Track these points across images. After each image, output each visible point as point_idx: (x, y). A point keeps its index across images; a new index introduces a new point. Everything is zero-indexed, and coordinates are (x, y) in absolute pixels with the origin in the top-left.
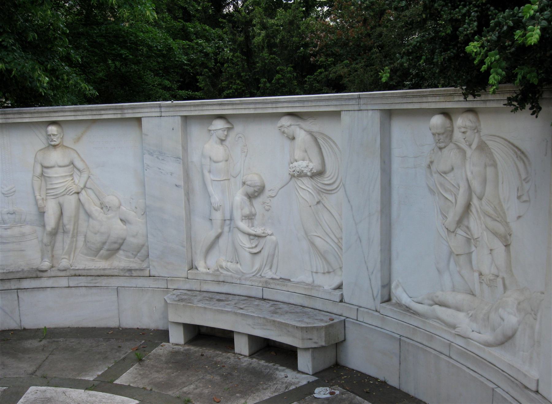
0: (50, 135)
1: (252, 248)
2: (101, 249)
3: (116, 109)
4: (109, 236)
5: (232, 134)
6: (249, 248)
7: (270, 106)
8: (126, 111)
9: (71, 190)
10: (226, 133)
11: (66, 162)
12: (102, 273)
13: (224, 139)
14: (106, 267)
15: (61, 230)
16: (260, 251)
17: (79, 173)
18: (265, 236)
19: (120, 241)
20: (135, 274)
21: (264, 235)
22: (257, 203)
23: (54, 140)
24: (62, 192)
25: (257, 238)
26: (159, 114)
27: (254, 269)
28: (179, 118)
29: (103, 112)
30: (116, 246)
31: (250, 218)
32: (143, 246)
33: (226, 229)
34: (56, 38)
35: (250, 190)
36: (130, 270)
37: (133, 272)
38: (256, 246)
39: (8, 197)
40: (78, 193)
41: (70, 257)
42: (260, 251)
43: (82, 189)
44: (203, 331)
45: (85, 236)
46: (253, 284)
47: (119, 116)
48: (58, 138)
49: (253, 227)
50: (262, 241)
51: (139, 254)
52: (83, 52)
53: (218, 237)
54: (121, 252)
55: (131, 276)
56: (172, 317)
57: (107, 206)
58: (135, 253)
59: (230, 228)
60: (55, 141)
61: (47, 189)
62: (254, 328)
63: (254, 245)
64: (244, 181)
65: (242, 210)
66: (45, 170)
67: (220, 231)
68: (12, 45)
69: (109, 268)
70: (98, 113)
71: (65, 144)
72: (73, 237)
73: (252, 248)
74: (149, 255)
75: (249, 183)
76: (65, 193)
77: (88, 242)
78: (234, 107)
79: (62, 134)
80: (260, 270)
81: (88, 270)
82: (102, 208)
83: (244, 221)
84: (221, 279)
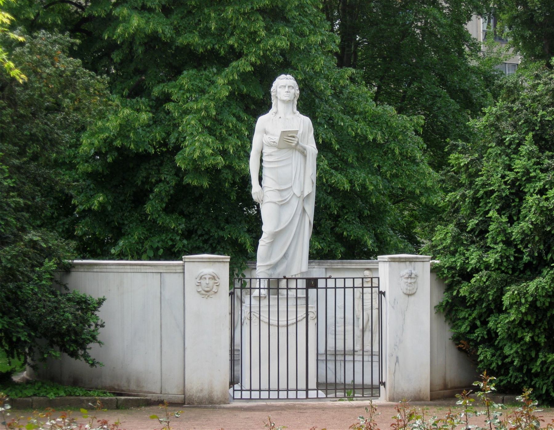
68: (353, 220)
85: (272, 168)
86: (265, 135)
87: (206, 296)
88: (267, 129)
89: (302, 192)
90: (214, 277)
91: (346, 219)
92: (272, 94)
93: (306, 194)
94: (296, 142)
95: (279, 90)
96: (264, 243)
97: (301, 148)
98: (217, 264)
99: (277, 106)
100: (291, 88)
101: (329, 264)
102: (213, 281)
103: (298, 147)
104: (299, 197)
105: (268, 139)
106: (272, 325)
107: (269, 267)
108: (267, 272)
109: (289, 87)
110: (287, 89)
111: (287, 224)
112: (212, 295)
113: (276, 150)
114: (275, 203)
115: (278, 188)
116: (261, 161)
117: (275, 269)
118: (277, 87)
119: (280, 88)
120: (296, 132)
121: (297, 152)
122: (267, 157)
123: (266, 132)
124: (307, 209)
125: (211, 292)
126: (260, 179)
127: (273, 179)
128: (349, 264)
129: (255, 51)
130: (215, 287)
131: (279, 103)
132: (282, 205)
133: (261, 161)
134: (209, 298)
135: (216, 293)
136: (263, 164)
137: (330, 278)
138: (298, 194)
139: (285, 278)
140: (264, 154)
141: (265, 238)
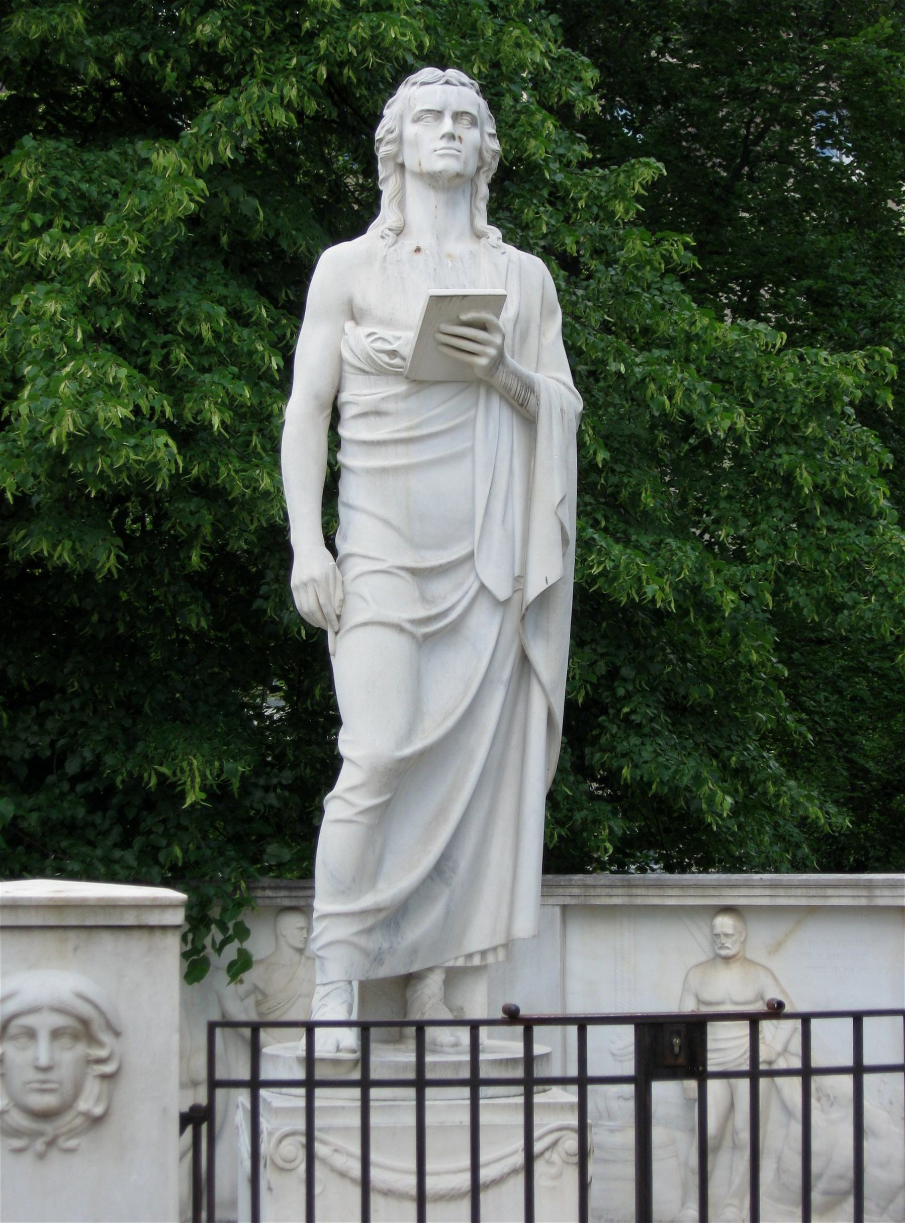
3: (856, 885)
8: (877, 892)
23: (727, 945)
24: (737, 1059)
29: (830, 892)
34: (754, 689)
39: (621, 1061)
45: (779, 1160)
47: (863, 902)
48: (736, 941)
52: (827, 699)
57: (829, 1096)
60: (728, 948)
68: (652, 720)
70: (820, 892)
71: (749, 955)
79: (744, 934)
85: (384, 470)
86: (349, 325)
87: (39, 1145)
88: (359, 301)
89: (520, 580)
90: (85, 1023)
91: (627, 719)
92: (382, 151)
93: (534, 589)
94: (492, 351)
95: (411, 130)
96: (347, 813)
97: (515, 385)
98: (108, 943)
99: (402, 205)
100: (466, 120)
101: (576, 891)
102: (81, 1049)
103: (501, 377)
104: (506, 603)
106: (388, 1193)
107: (370, 922)
108: (362, 941)
109: (457, 116)
111: (450, 723)
112: (73, 1133)
113: (402, 388)
114: (398, 628)
115: (410, 563)
116: (335, 442)
117: (397, 926)
118: (402, 117)
119: (417, 120)
120: (496, 302)
121: (496, 402)
122: (361, 422)
123: (354, 314)
125: (69, 1120)
127: (386, 522)
128: (652, 892)
129: (300, 68)
130: (92, 1087)
131: (413, 188)
132: (427, 637)
133: (335, 442)
134: (54, 1154)
135: (96, 1121)
136: (340, 457)
137: (776, 1011)
138: (502, 590)
139: (512, 1016)
140: (347, 413)
141: (352, 789)
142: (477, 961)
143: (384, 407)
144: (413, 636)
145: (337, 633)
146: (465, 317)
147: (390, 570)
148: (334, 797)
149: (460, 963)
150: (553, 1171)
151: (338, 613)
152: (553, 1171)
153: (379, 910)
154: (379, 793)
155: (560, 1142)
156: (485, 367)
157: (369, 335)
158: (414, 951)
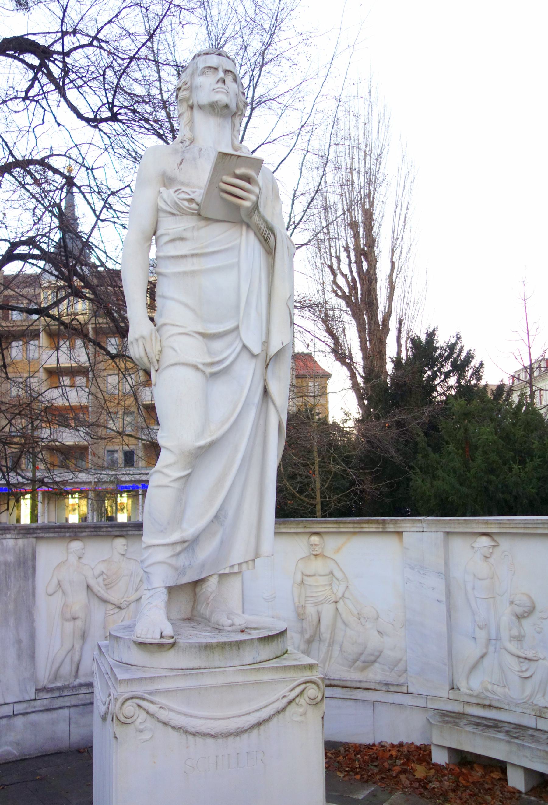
0: (312, 545)
1: (522, 672)
2: (357, 660)
4: (366, 647)
5: (498, 551)
6: (519, 672)
7: (541, 526)
9: (327, 598)
10: (491, 550)
11: (327, 572)
12: (358, 685)
13: (488, 556)
14: (361, 679)
15: (317, 638)
16: (531, 676)
17: (338, 583)
18: (537, 660)
19: (377, 654)
20: (392, 689)
21: (535, 659)
22: (527, 624)
25: (527, 661)
26: (421, 530)
27: (525, 695)
28: (442, 533)
30: (373, 658)
31: (519, 638)
32: (401, 660)
33: (491, 649)
35: (519, 610)
36: (387, 684)
37: (390, 687)
38: (526, 670)
40: (336, 602)
41: (324, 666)
42: (531, 676)
43: (341, 598)
44: (469, 758)
45: (341, 646)
46: (525, 711)
47: (380, 530)
49: (522, 649)
50: (533, 665)
51: (396, 669)
53: (483, 657)
54: (377, 665)
55: (388, 691)
56: (435, 741)
58: (391, 667)
59: (496, 648)
61: (306, 597)
62: (532, 761)
63: (524, 669)
64: (511, 600)
65: (510, 630)
66: (305, 578)
67: (484, 650)
69: (365, 680)
71: (325, 554)
72: (329, 645)
73: (522, 672)
74: (407, 670)
75: (517, 602)
76: (324, 601)
77: (344, 652)
78: (502, 525)
80: (531, 696)
81: (343, 680)
82: (359, 619)
83: (512, 642)
84: (487, 703)
85: (185, 273)
89: (266, 343)
103: (256, 218)
105: (174, 196)
107: (179, 548)
108: (173, 561)
110: (221, 74)
111: (227, 426)
114: (196, 368)
124: (273, 389)
126: (152, 307)
127: (186, 305)
141: (168, 466)
142: (236, 569)
143: (185, 235)
144: (204, 373)
145: (157, 371)
146: (238, 171)
147: (190, 333)
148: (156, 472)
149: (227, 571)
150: (301, 710)
151: (158, 358)
152: (301, 710)
153: (184, 542)
154: (185, 469)
155: (305, 691)
156: (248, 208)
157: (176, 191)
158: (203, 566)
